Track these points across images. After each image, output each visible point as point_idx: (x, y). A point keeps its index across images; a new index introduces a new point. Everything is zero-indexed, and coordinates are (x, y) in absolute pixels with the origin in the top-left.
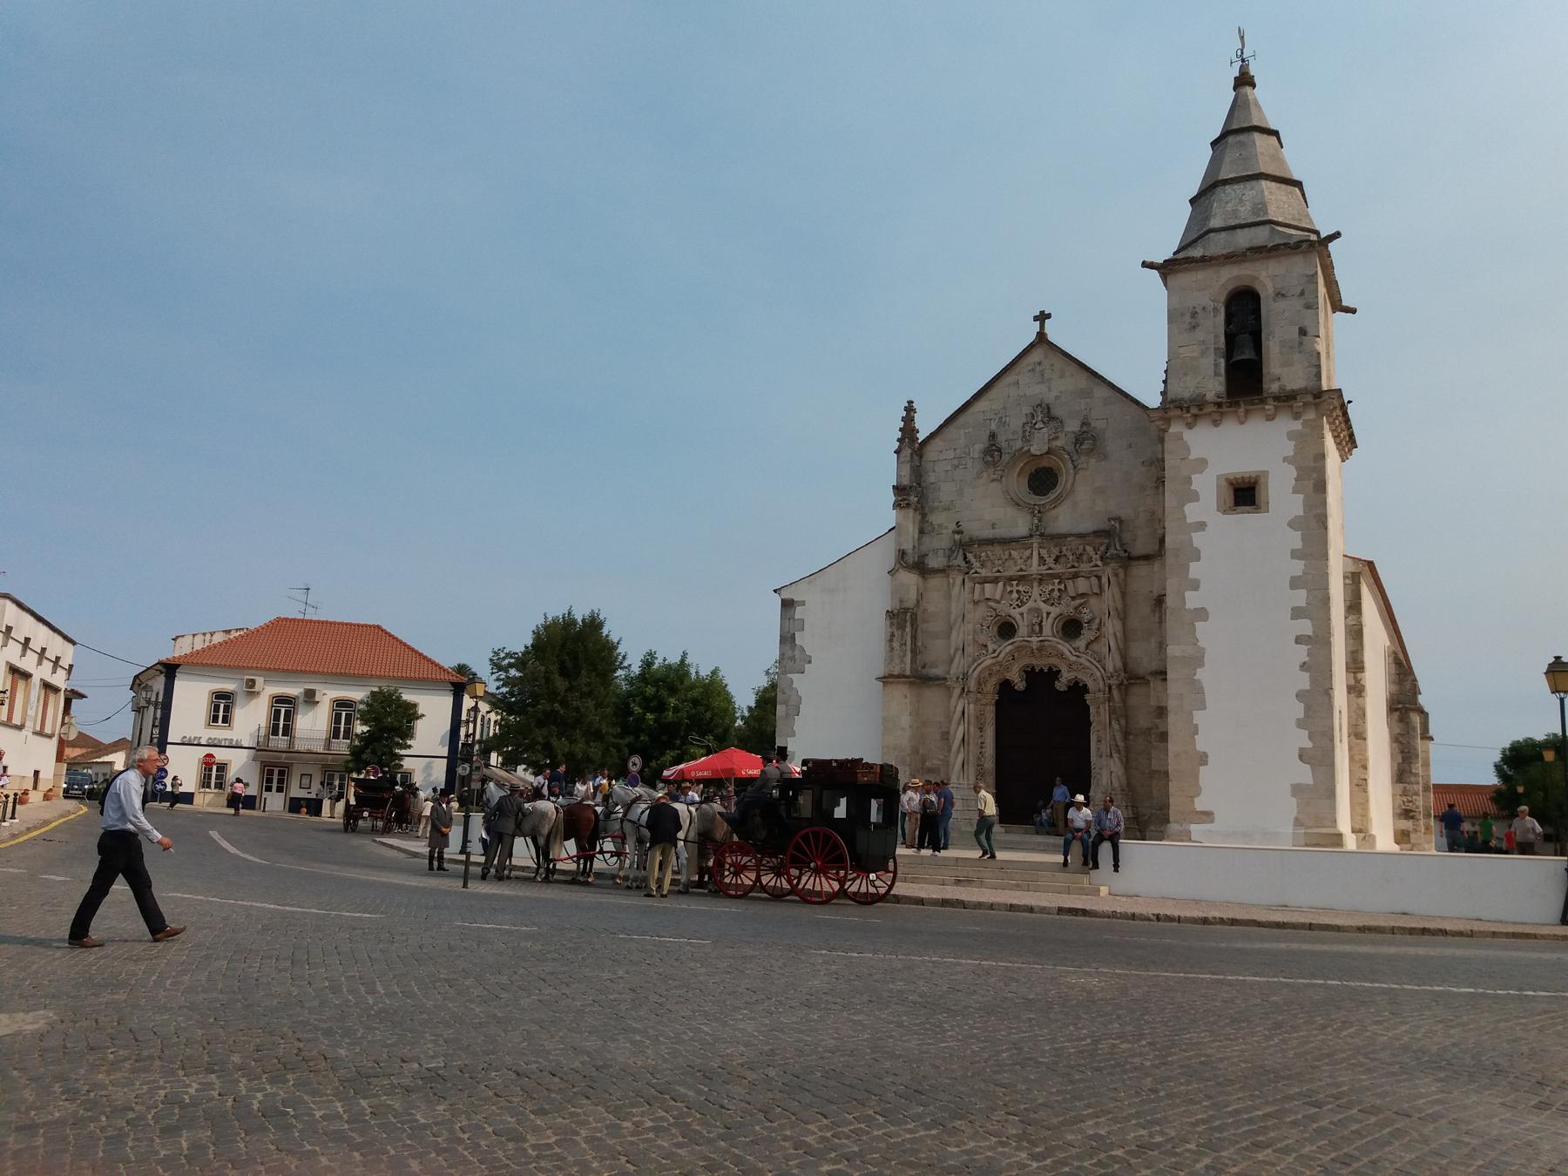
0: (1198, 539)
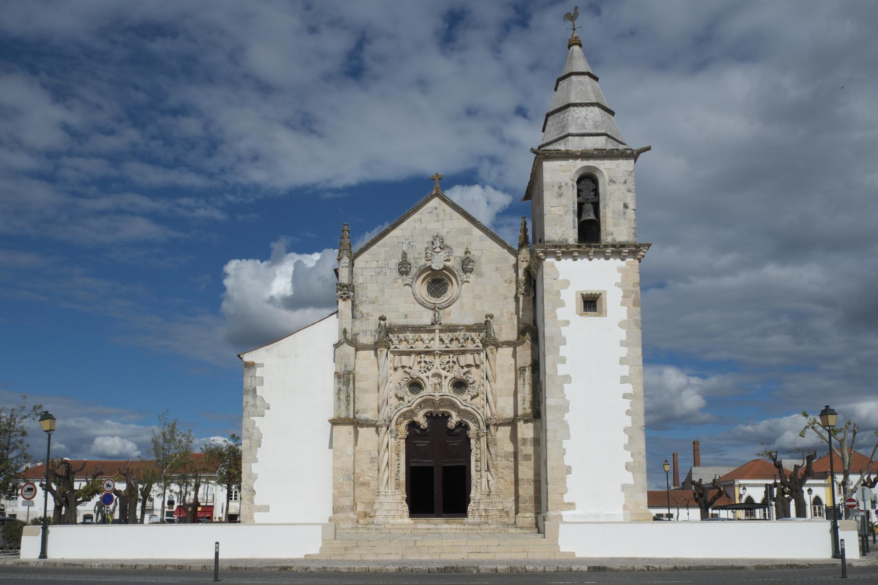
0: (565, 331)
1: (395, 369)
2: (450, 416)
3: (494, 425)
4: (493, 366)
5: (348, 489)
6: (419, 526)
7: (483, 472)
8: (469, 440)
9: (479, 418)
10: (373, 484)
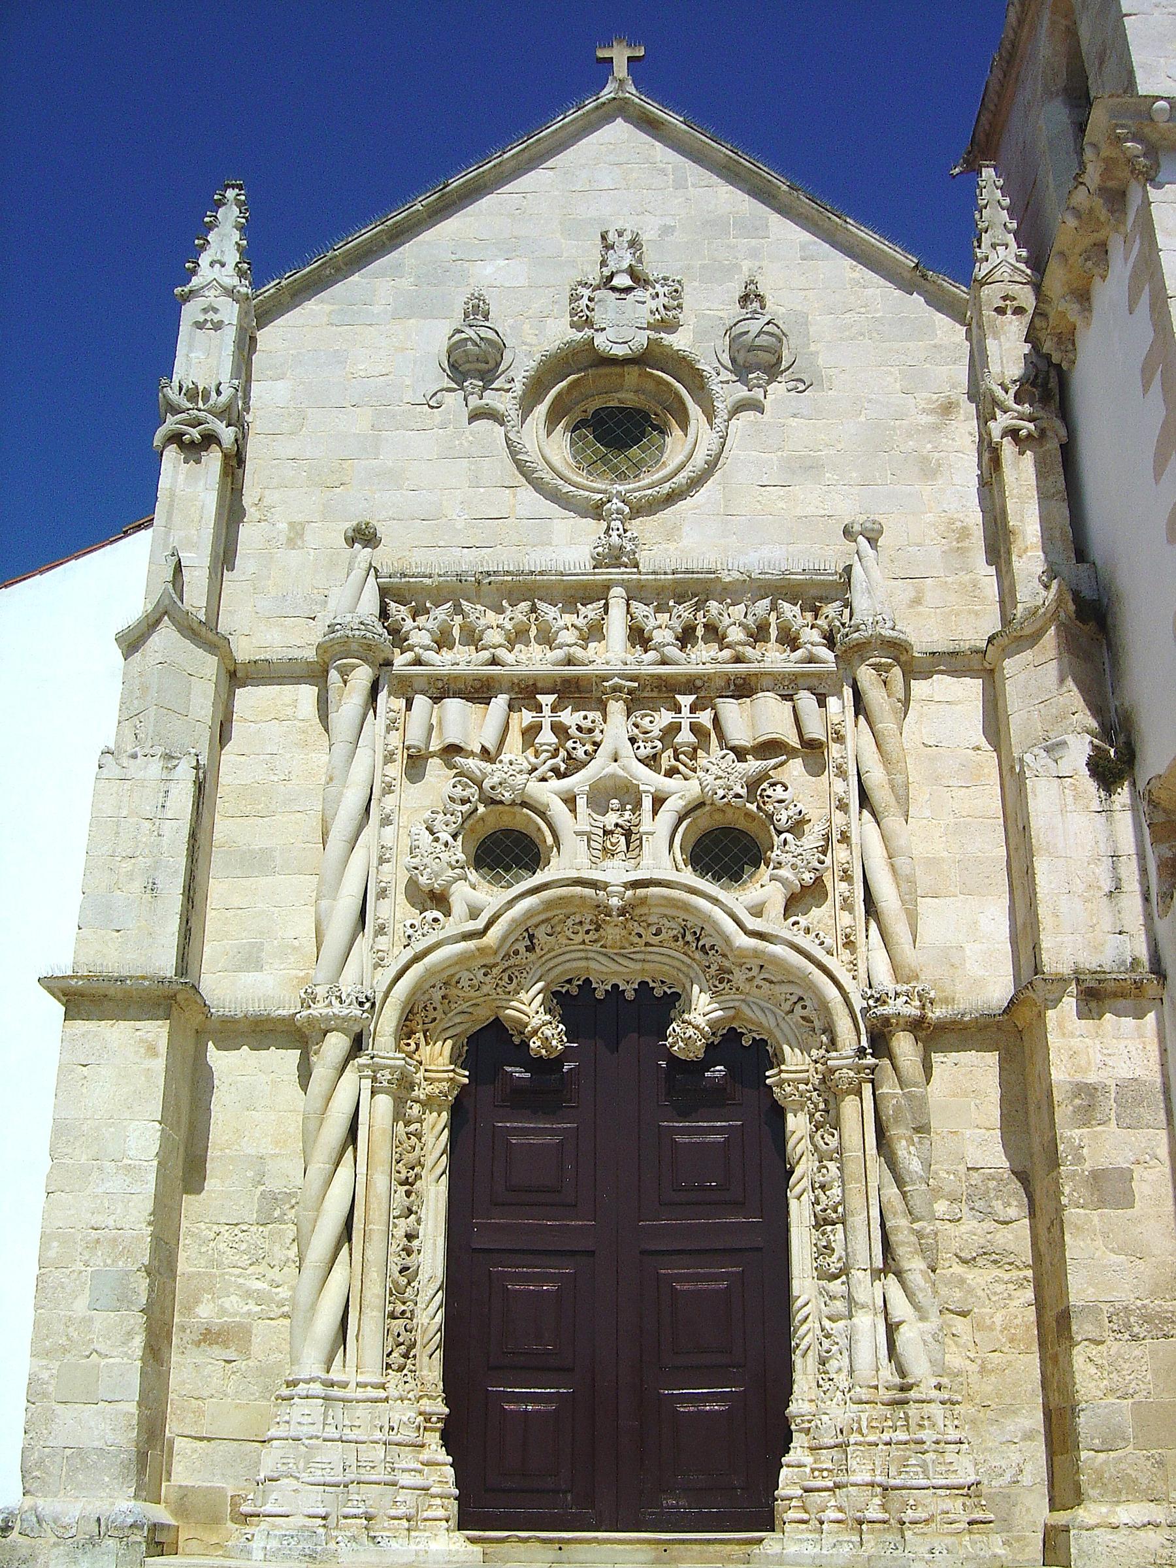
3: (917, 1026)
4: (891, 745)
7: (860, 1277)
8: (778, 1114)
10: (267, 1338)
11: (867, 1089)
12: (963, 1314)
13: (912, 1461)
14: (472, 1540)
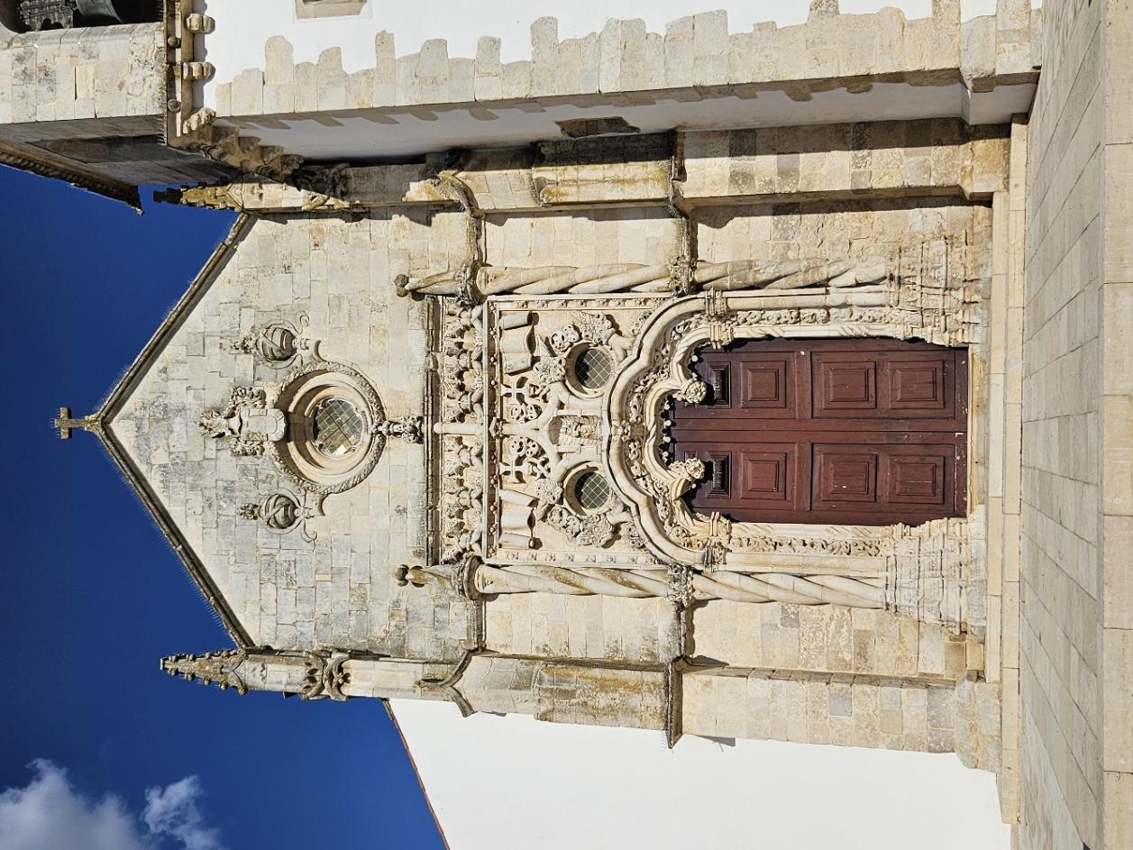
0: (406, 46)
1: (537, 544)
2: (668, 396)
4: (532, 275)
5: (868, 700)
6: (995, 489)
7: (829, 300)
8: (738, 343)
9: (673, 313)
10: (864, 621)
11: (726, 294)
12: (850, 244)
13: (932, 275)
14: (972, 510)
